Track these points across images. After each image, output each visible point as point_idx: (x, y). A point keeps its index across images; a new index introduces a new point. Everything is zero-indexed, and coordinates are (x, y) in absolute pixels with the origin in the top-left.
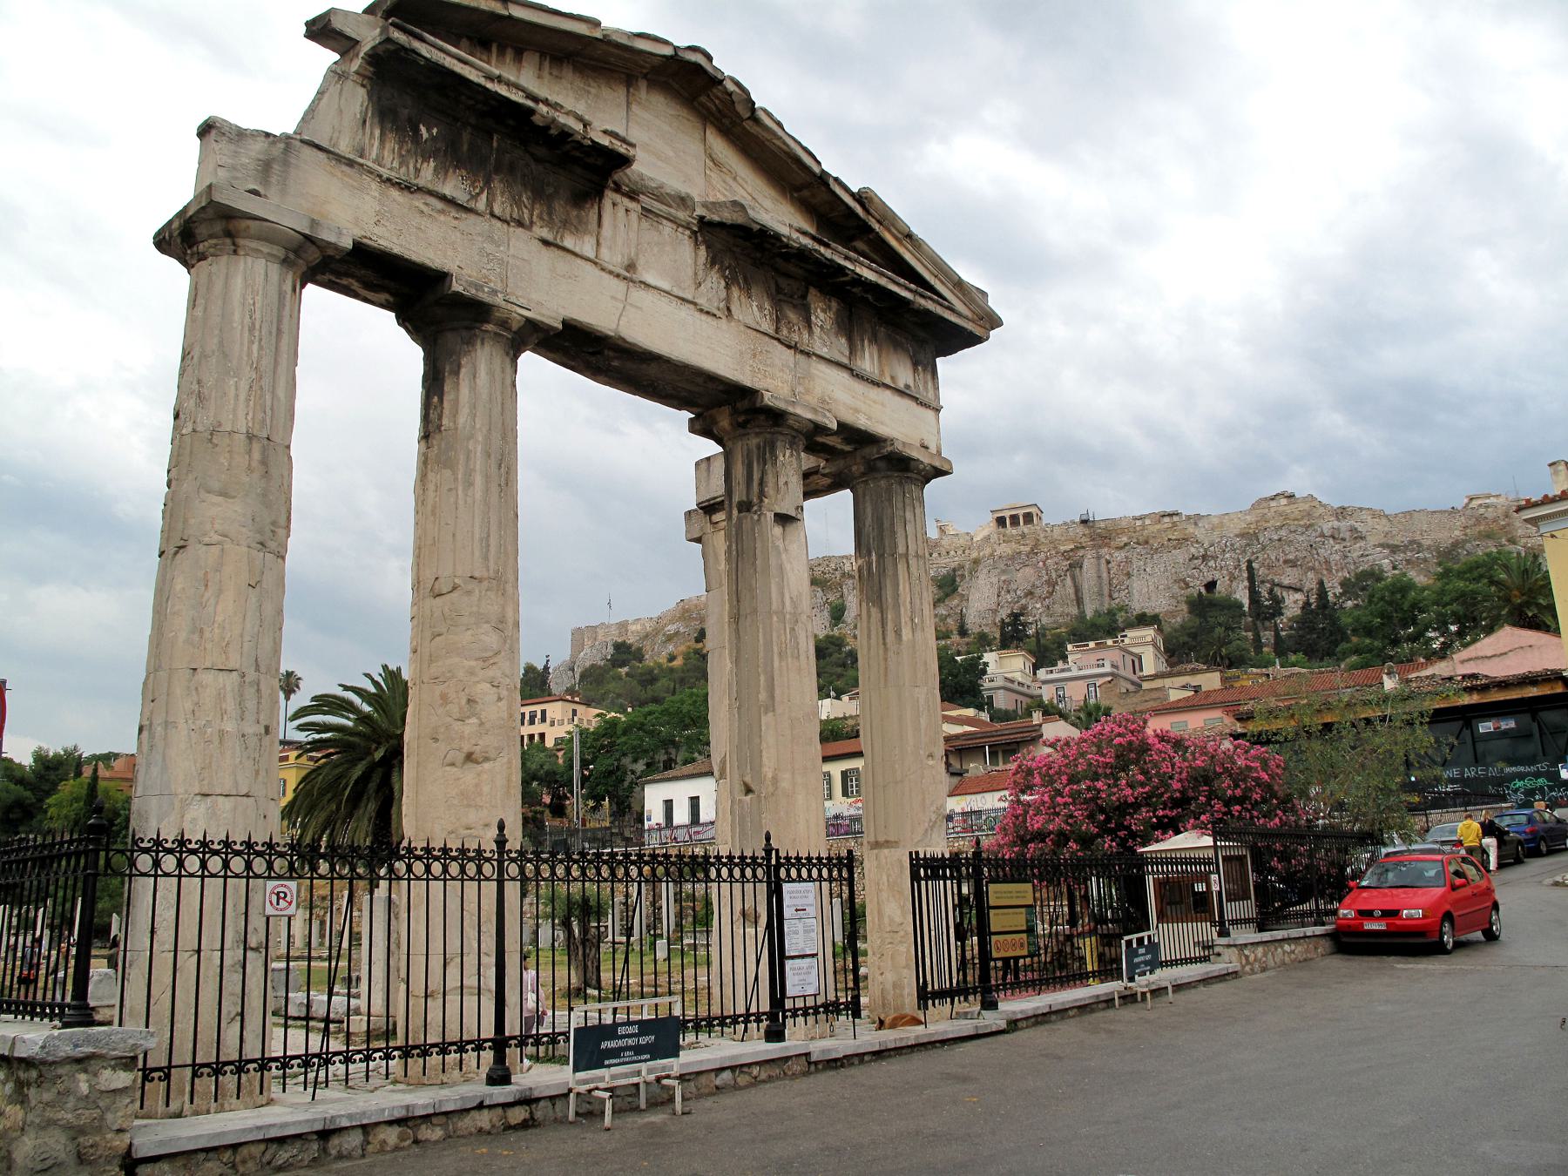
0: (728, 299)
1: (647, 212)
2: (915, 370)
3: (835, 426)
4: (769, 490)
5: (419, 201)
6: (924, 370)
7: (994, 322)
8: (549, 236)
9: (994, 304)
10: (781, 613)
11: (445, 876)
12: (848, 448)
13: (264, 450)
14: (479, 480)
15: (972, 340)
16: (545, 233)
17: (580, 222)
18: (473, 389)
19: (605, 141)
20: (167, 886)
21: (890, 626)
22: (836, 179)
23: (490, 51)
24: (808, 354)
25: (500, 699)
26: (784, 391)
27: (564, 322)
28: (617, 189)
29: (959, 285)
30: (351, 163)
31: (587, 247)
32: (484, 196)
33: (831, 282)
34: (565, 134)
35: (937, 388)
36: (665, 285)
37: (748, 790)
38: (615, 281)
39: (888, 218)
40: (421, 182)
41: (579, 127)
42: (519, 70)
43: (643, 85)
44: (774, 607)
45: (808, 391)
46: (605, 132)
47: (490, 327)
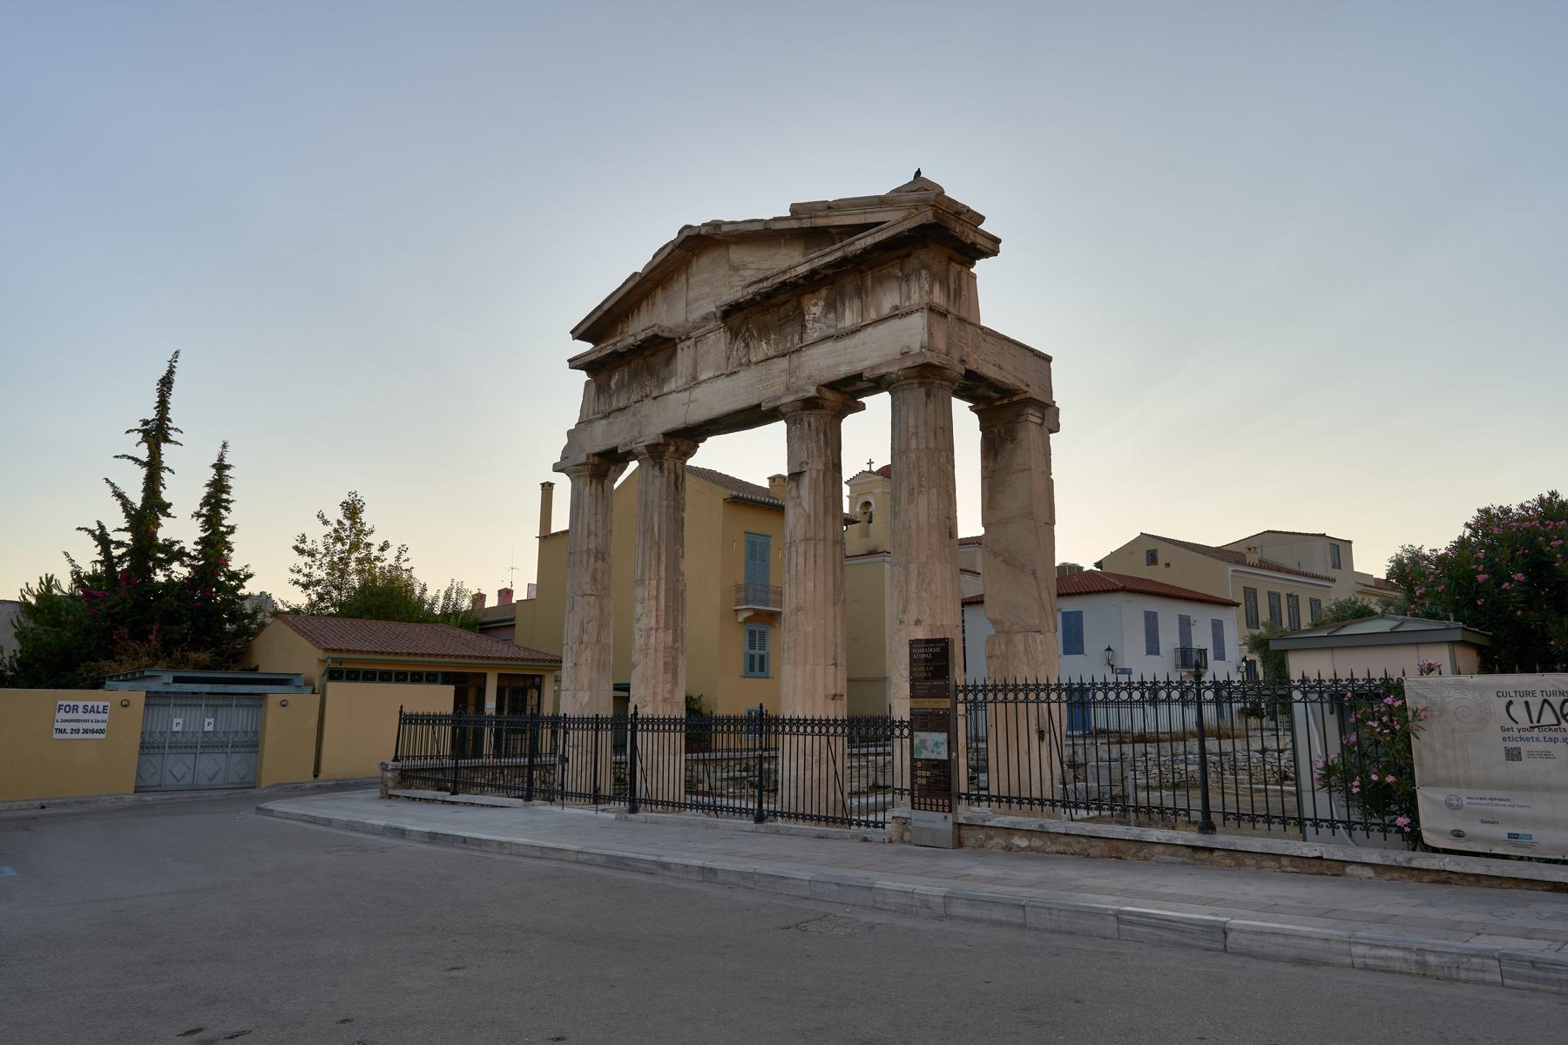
19: (642, 336)
22: (775, 219)
31: (672, 385)
36: (710, 374)
40: (615, 406)
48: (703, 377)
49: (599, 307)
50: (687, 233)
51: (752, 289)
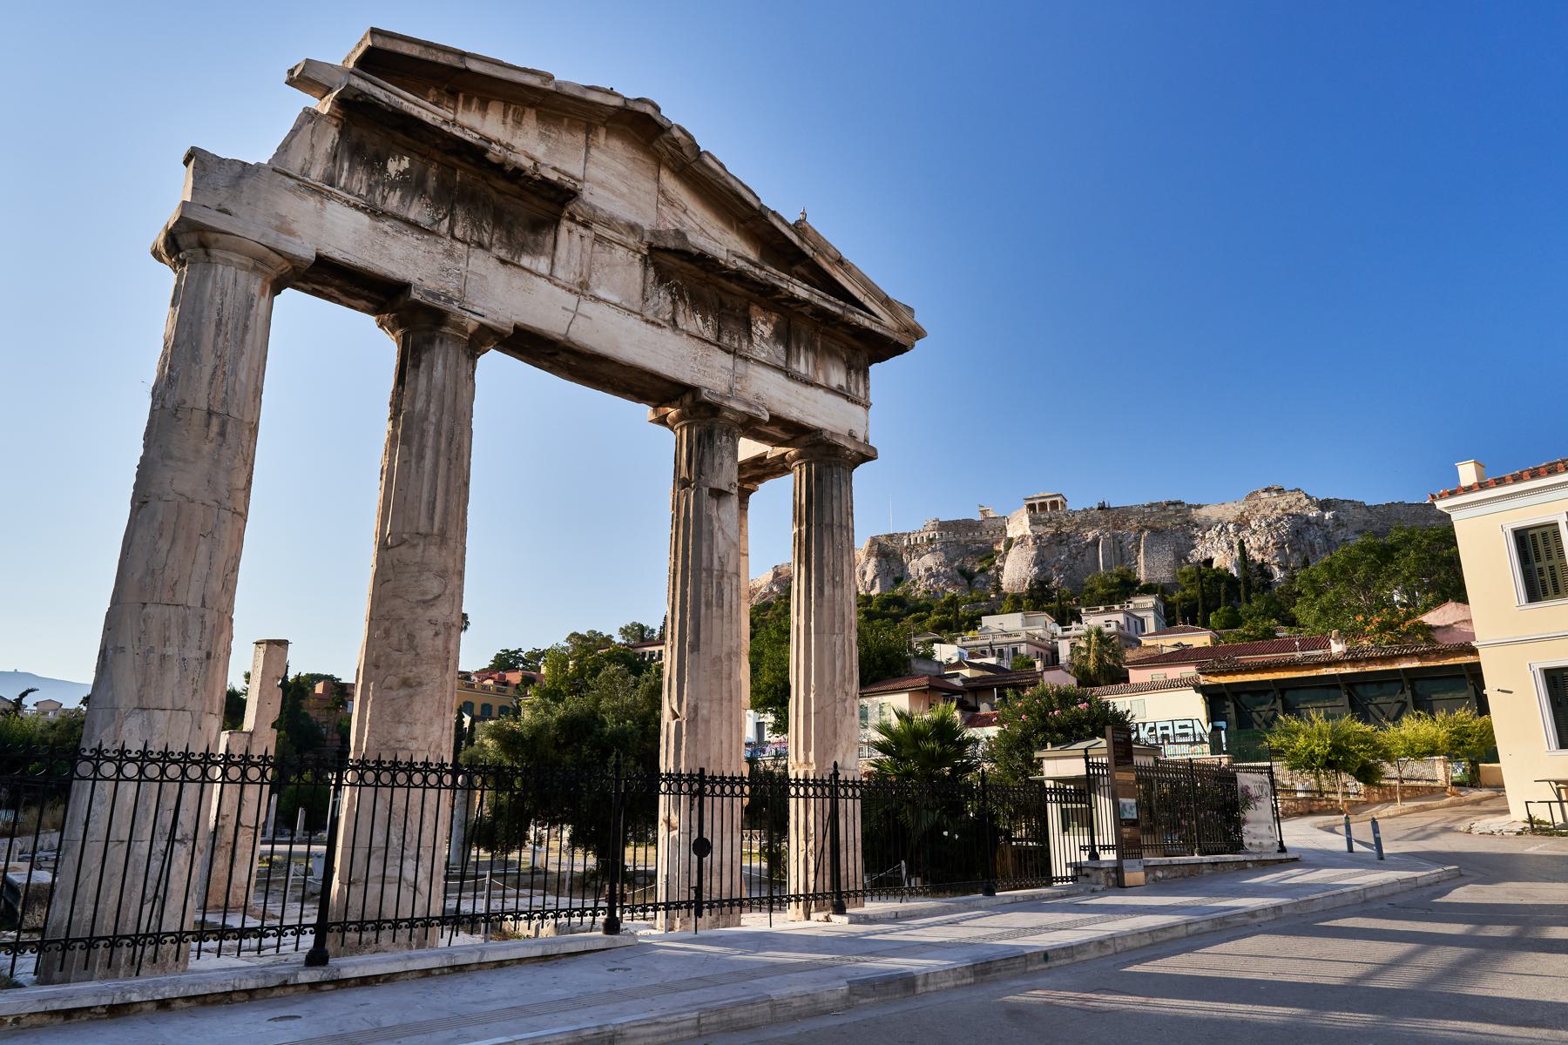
0: (674, 313)
1: (599, 239)
2: (848, 374)
3: (767, 418)
4: (706, 469)
5: (385, 225)
6: (857, 373)
7: (917, 333)
8: (508, 257)
9: (920, 319)
10: (710, 570)
11: (439, 785)
13: (223, 425)
14: (429, 454)
15: (900, 349)
16: (503, 253)
17: (537, 245)
18: (430, 378)
19: (553, 176)
22: (774, 213)
23: (457, 100)
24: (746, 359)
25: (437, 634)
26: (722, 387)
27: (516, 327)
28: (572, 218)
29: (887, 302)
30: (317, 191)
31: (542, 265)
32: (446, 221)
33: (770, 297)
34: (518, 171)
35: (867, 388)
36: (615, 299)
38: (568, 295)
39: (821, 246)
41: (528, 164)
42: (484, 117)
43: (602, 132)
44: (704, 565)
45: (743, 389)
46: (554, 169)
47: (447, 330)
48: (601, 293)
49: (463, 55)
50: (649, 110)
51: (741, 263)
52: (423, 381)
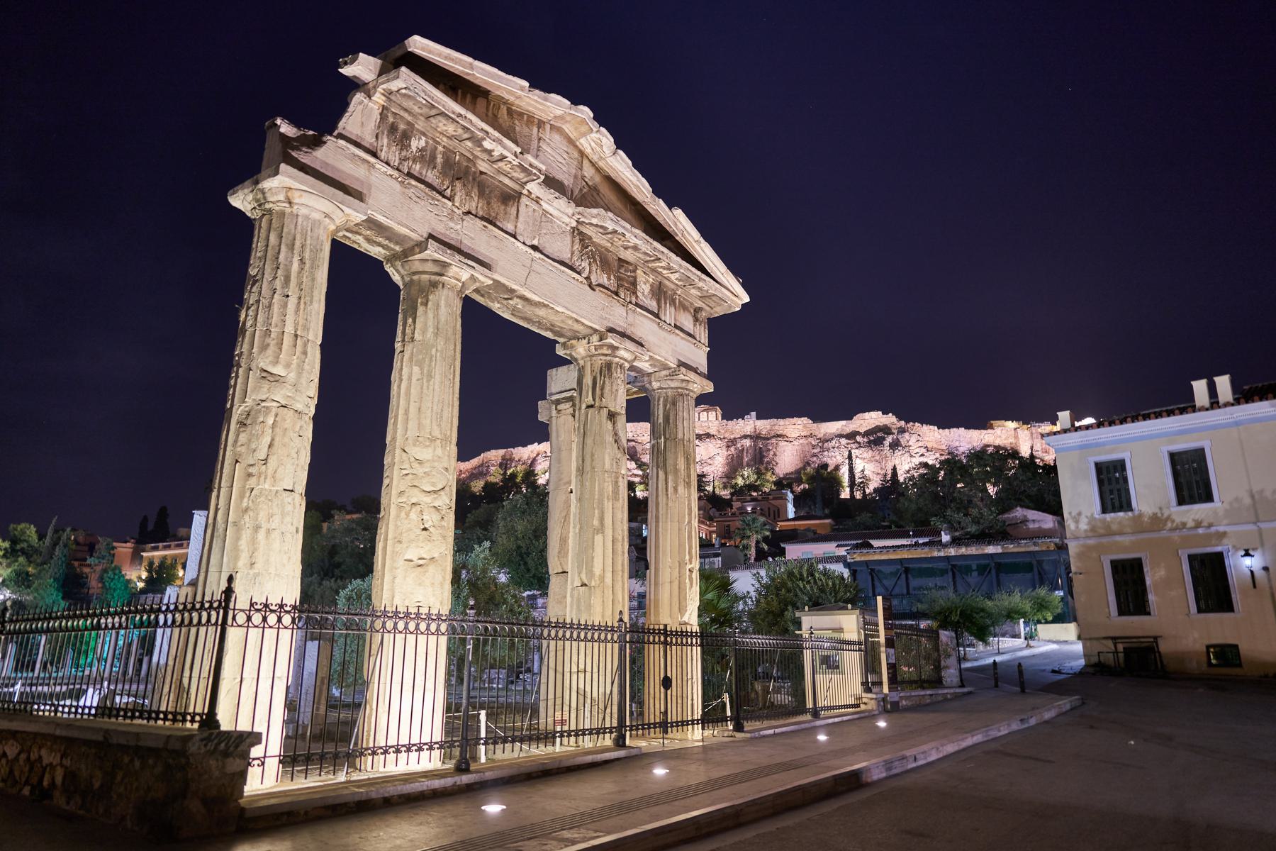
12: (651, 370)
13: (305, 345)
14: (438, 377)
18: (436, 316)
20: (254, 634)
21: (670, 484)
37: (584, 585)
52: (431, 315)
